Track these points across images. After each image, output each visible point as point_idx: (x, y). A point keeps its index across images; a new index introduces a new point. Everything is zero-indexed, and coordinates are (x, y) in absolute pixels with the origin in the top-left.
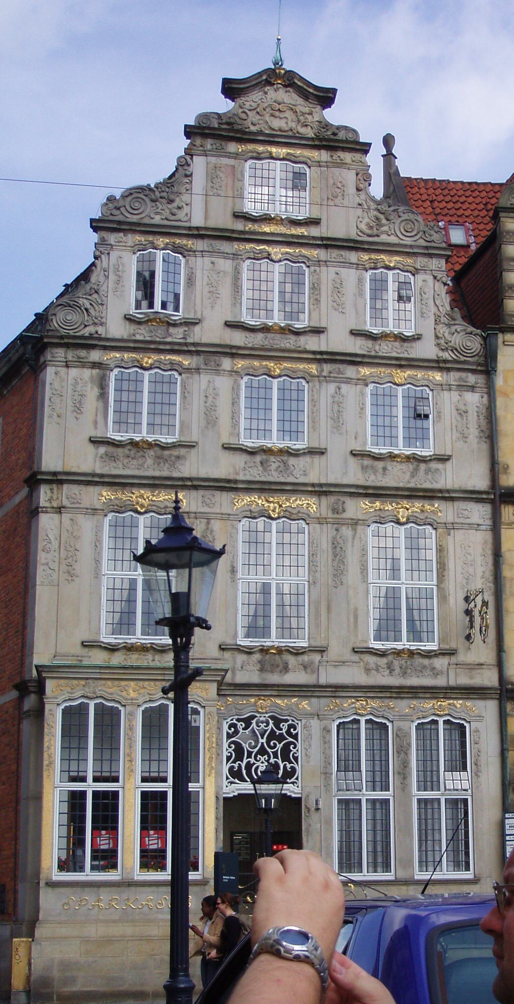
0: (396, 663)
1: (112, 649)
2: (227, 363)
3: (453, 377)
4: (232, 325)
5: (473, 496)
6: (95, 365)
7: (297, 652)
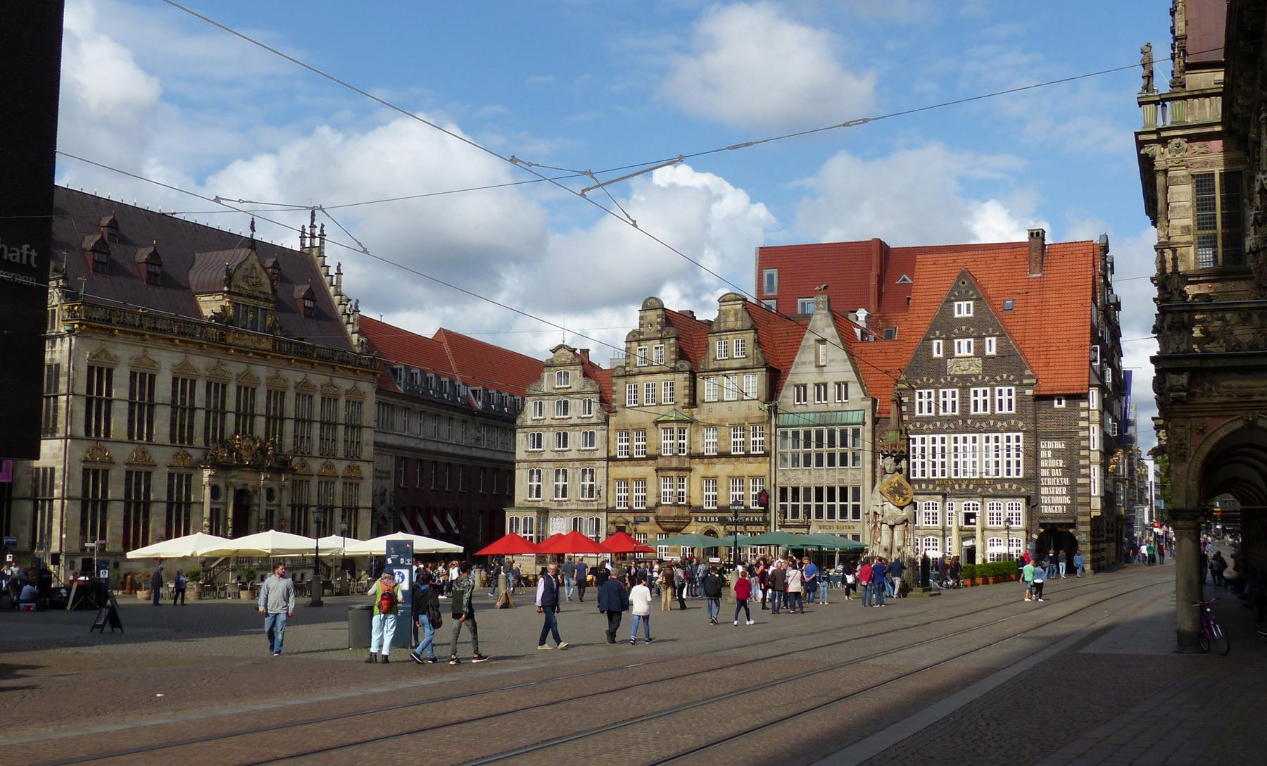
1: (529, 501)
2: (551, 429)
3: (599, 427)
4: (553, 419)
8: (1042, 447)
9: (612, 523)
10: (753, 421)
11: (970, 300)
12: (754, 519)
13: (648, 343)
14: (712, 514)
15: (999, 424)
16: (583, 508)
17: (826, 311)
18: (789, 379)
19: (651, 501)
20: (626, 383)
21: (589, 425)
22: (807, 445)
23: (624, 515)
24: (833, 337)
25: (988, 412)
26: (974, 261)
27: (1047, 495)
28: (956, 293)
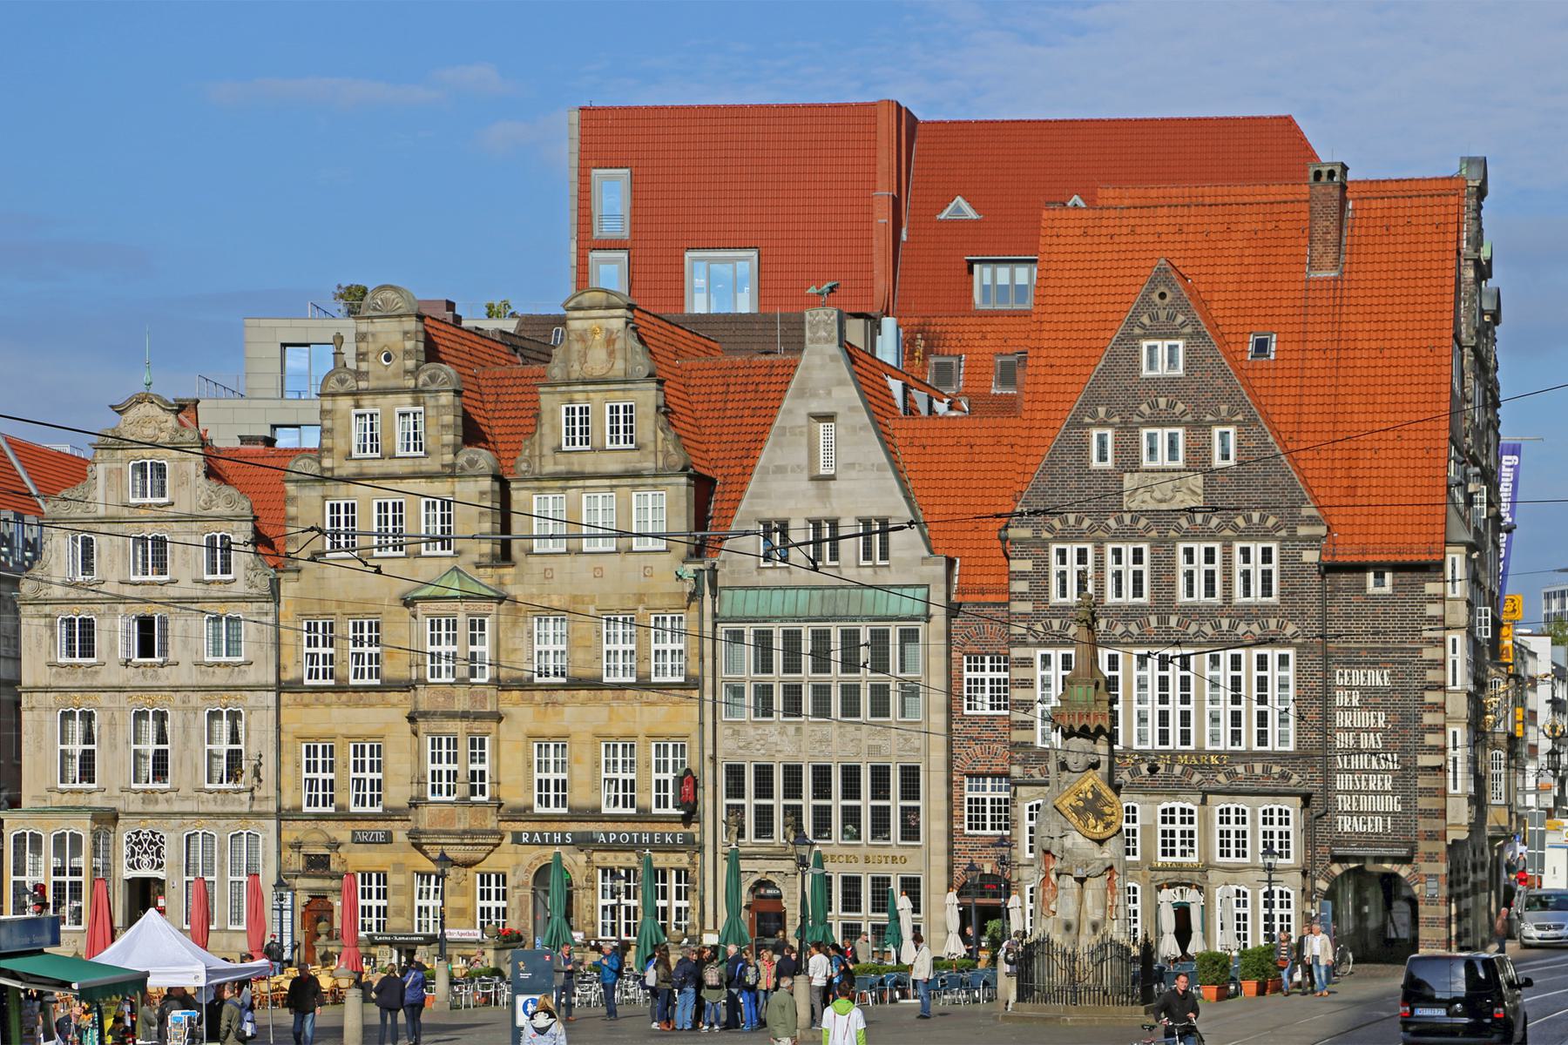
0: (219, 796)
1: (63, 792)
2: (121, 608)
5: (265, 688)
6: (46, 616)
7: (164, 792)
8: (1339, 681)
9: (292, 846)
10: (657, 603)
11: (1177, 336)
12: (662, 836)
13: (380, 400)
14: (555, 826)
15: (1242, 628)
16: (212, 808)
18: (743, 506)
19: (397, 795)
20: (324, 498)
21: (227, 600)
22: (792, 665)
23: (323, 825)
24: (852, 409)
25: (1217, 599)
26: (1181, 231)
27: (1348, 792)
28: (1145, 320)
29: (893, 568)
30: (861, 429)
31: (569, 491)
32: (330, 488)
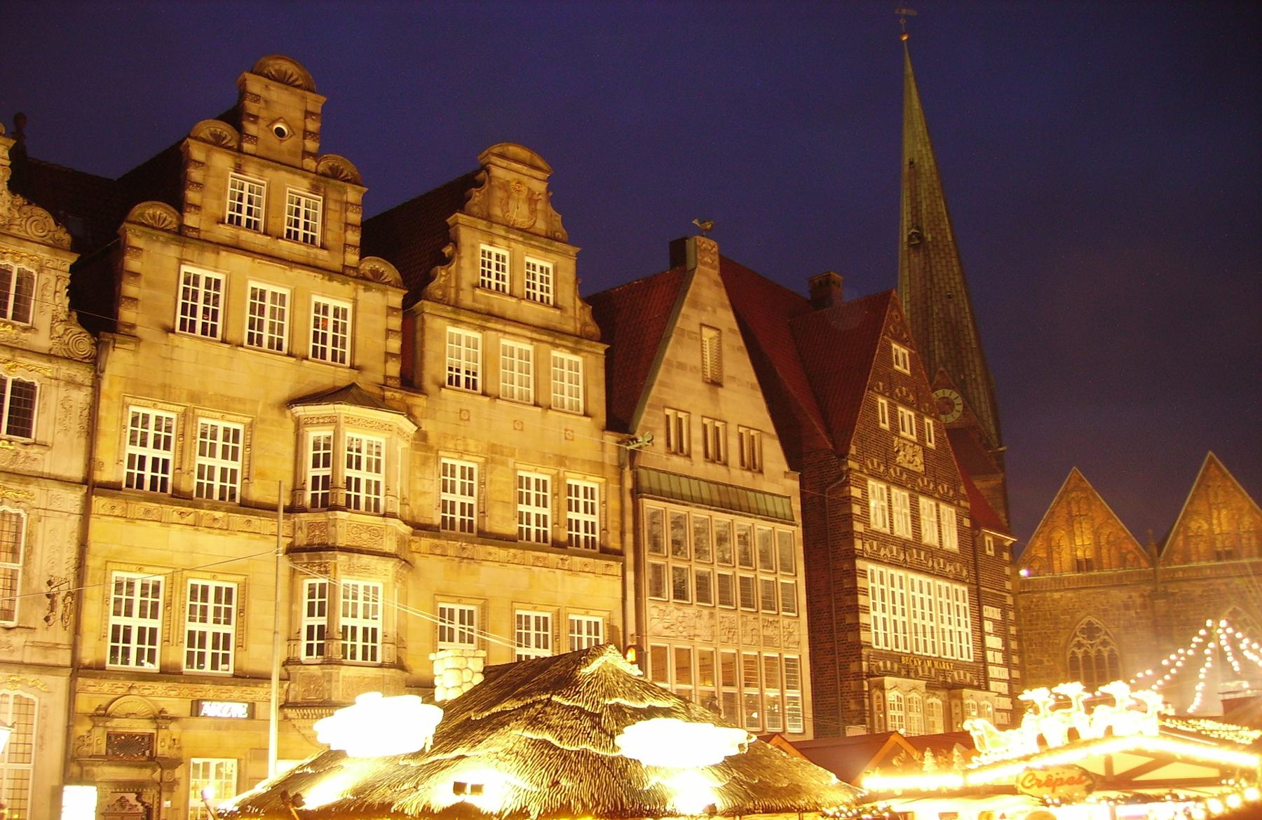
17: (715, 274)
29: (765, 476)
30: (738, 349)
31: (490, 333)
32: (190, 252)
